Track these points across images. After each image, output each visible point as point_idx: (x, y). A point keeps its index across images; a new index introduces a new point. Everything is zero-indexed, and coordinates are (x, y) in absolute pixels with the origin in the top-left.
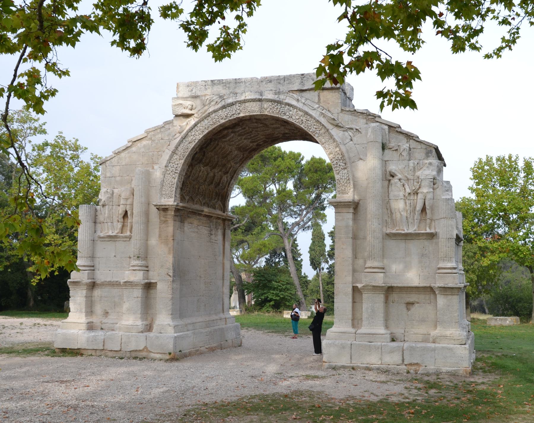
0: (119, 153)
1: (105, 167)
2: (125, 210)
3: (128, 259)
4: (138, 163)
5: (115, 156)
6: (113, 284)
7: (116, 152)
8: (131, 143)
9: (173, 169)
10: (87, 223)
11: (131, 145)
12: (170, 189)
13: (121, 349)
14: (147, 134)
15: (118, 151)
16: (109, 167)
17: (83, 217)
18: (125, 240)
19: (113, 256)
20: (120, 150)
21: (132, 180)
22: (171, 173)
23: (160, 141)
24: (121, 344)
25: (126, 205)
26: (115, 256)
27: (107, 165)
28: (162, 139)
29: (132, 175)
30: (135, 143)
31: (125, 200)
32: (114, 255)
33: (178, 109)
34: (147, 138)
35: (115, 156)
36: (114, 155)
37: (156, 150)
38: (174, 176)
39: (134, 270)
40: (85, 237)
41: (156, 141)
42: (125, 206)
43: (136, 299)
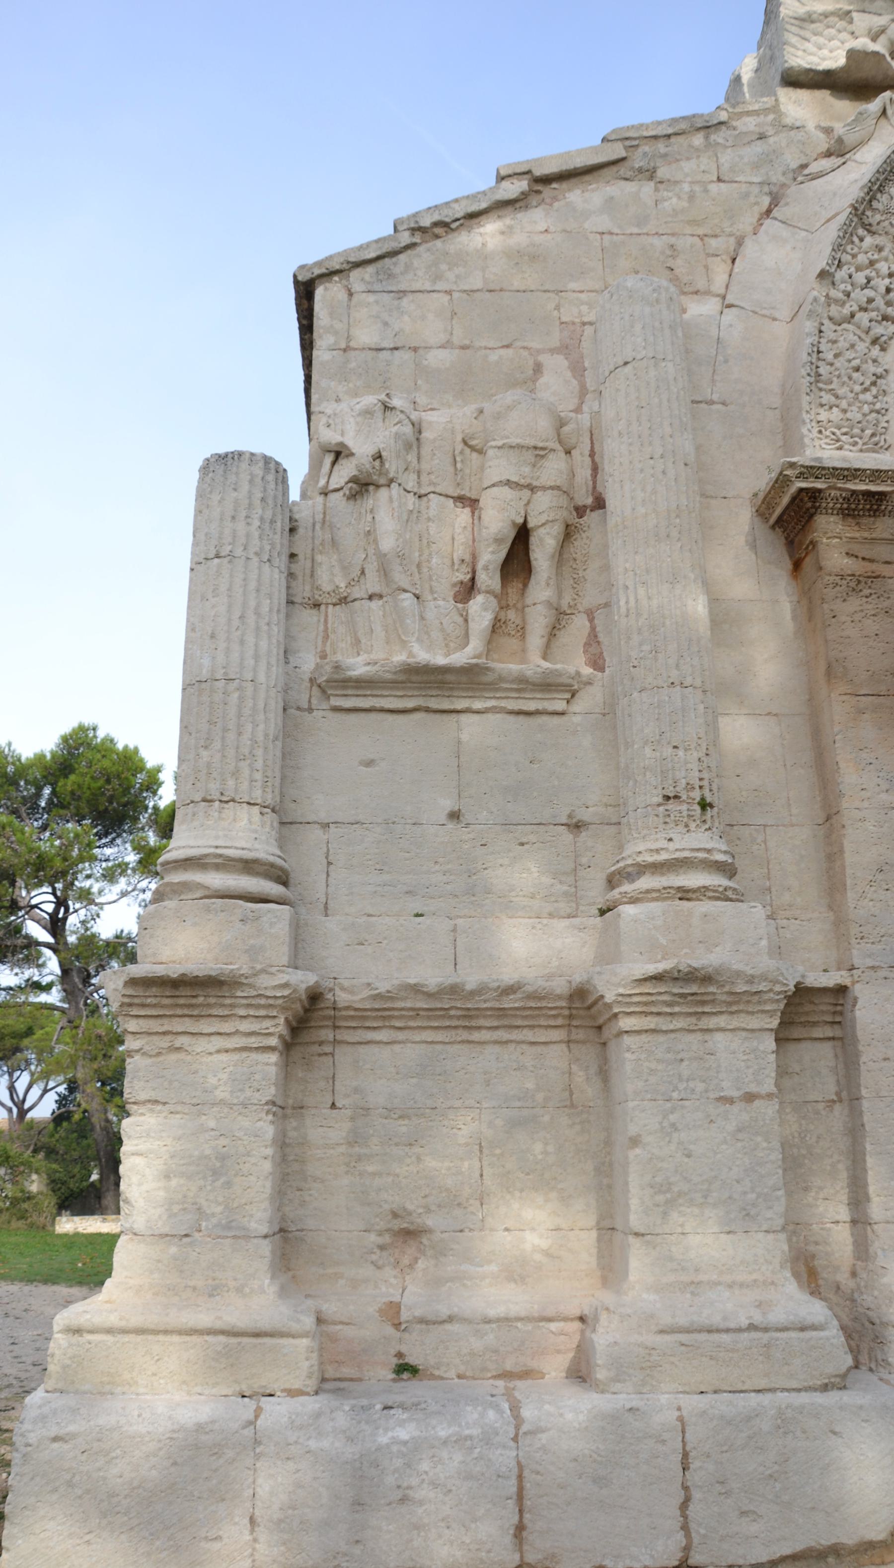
0: (438, 230)
1: (342, 295)
2: (521, 520)
3: (567, 837)
4: (573, 285)
5: (412, 246)
6: (469, 1014)
7: (426, 222)
8: (521, 186)
9: (869, 293)
10: (266, 567)
11: (524, 195)
12: (868, 397)
13: (687, 1549)
14: (626, 148)
15: (436, 217)
16: (371, 298)
17: (241, 526)
18: (531, 706)
19: (443, 819)
20: (446, 215)
21: (538, 369)
22: (863, 318)
23: (714, 188)
24: (684, 1506)
25: (532, 489)
26: (455, 816)
27: (357, 287)
28: (719, 180)
29: (535, 345)
30: (547, 191)
31: (529, 456)
32: (448, 804)
33: (821, 40)
34: (623, 170)
35: (412, 246)
36: (405, 238)
37: (688, 230)
38: (878, 330)
39: (685, 894)
40: (256, 657)
41: (686, 187)
42: (526, 493)
43: (739, 1114)
